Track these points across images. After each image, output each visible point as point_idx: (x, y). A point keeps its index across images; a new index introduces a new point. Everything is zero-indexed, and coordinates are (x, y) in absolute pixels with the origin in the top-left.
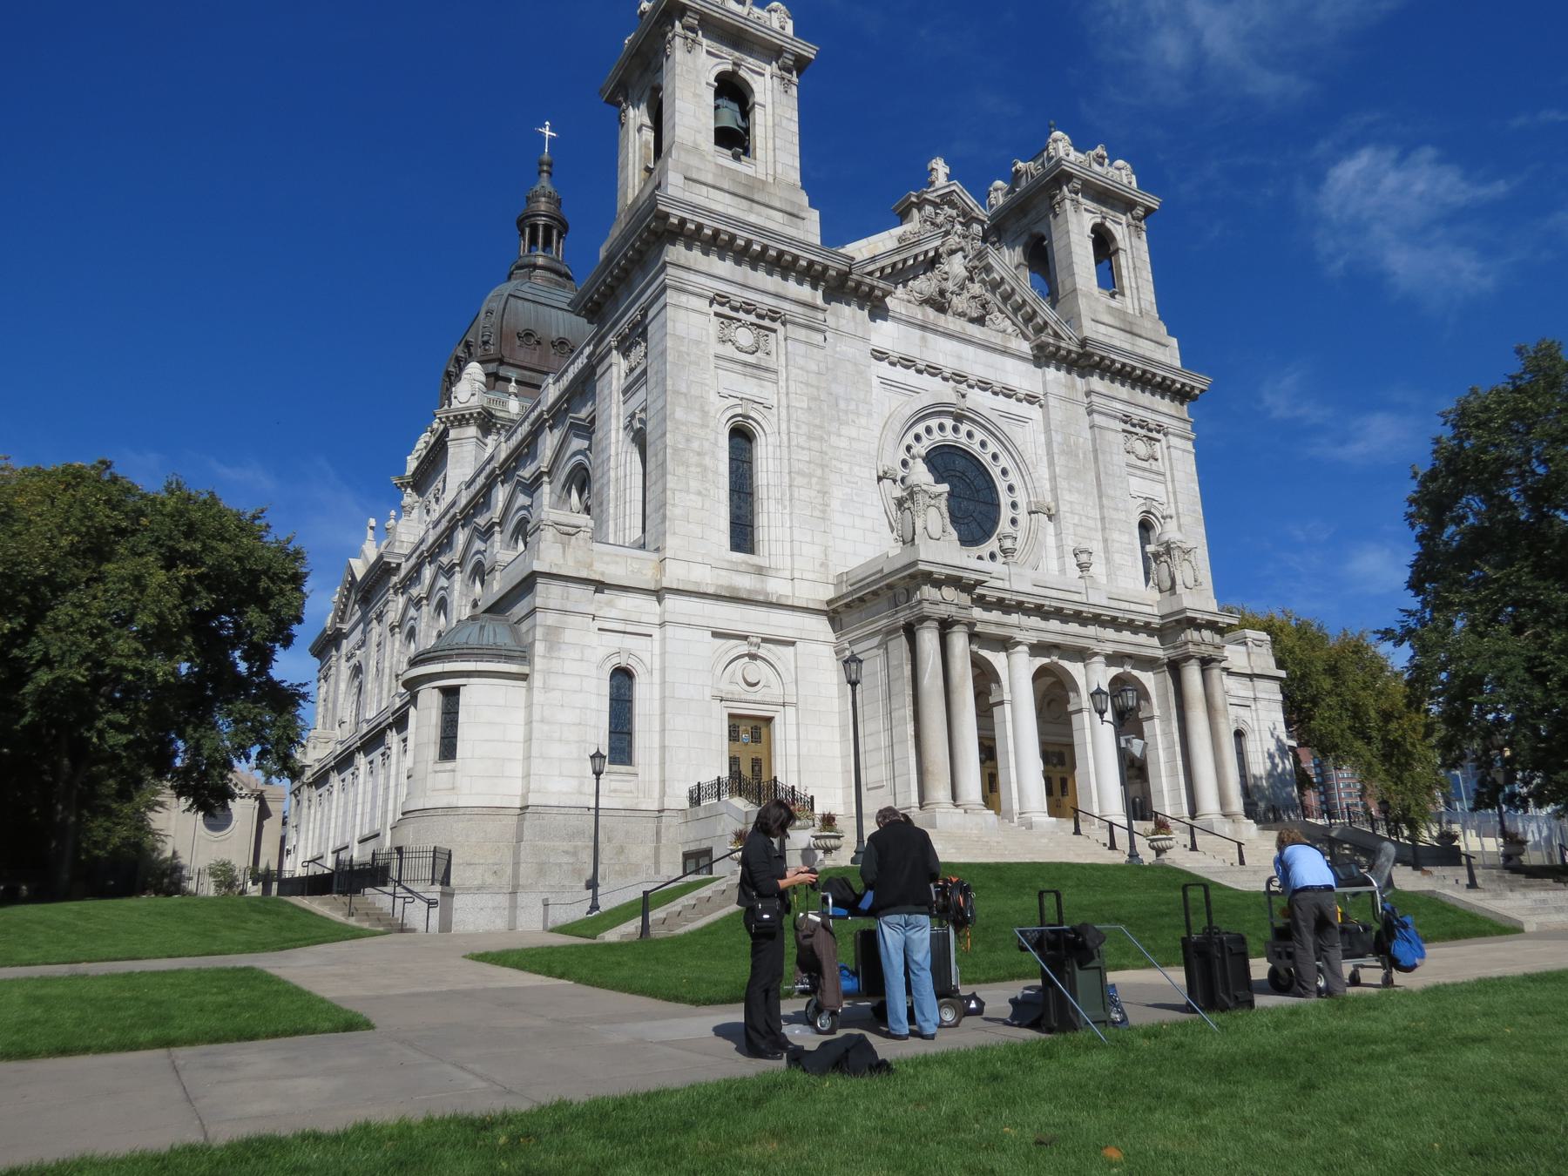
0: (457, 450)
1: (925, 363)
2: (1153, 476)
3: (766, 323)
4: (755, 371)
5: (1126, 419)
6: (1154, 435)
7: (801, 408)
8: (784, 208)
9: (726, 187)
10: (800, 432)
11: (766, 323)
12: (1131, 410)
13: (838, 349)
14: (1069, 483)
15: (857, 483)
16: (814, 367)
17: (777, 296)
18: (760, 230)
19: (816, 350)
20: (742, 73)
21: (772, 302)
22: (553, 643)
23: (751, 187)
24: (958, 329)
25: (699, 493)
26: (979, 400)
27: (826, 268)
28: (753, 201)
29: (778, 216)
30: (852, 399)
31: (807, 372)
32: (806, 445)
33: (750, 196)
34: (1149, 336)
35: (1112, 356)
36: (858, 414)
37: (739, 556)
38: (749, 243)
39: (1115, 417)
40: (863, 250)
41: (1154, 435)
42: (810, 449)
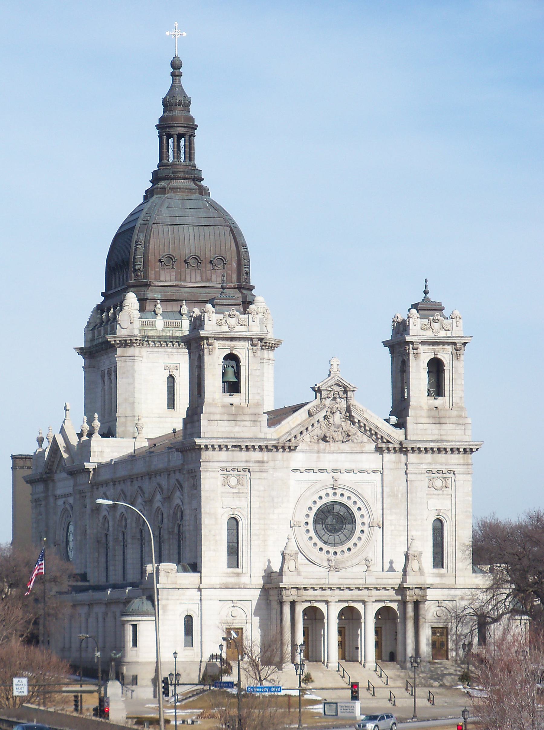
0: (123, 364)
3: (242, 473)
5: (429, 471)
6: (448, 475)
11: (242, 473)
12: (433, 466)
13: (275, 475)
16: (262, 488)
20: (234, 352)
21: (244, 465)
22: (165, 611)
25: (214, 550)
26: (345, 479)
34: (451, 423)
35: (418, 446)
37: (231, 570)
41: (448, 475)
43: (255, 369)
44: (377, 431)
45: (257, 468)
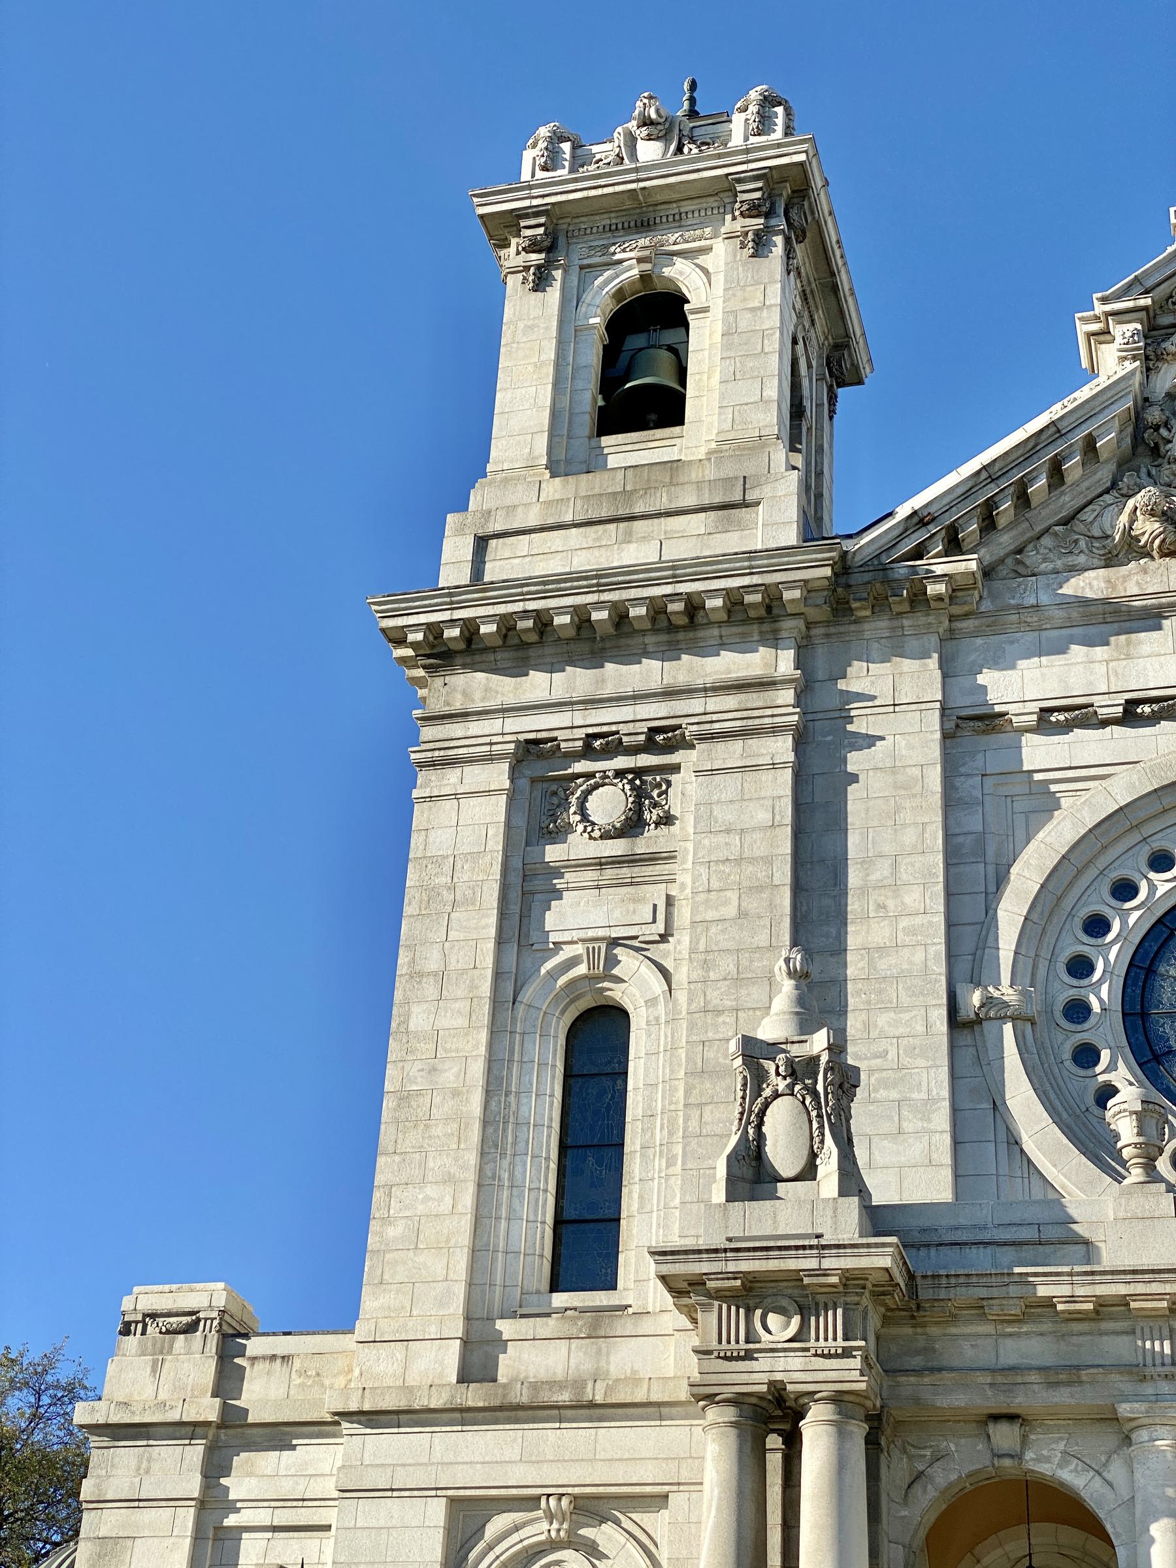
1: (1121, 699)
4: (625, 872)
8: (706, 500)
9: (568, 518)
10: (712, 975)
17: (670, 693)
18: (599, 579)
19: (766, 777)
23: (626, 495)
28: (632, 518)
29: (697, 522)
33: (621, 512)
43: (753, 310)
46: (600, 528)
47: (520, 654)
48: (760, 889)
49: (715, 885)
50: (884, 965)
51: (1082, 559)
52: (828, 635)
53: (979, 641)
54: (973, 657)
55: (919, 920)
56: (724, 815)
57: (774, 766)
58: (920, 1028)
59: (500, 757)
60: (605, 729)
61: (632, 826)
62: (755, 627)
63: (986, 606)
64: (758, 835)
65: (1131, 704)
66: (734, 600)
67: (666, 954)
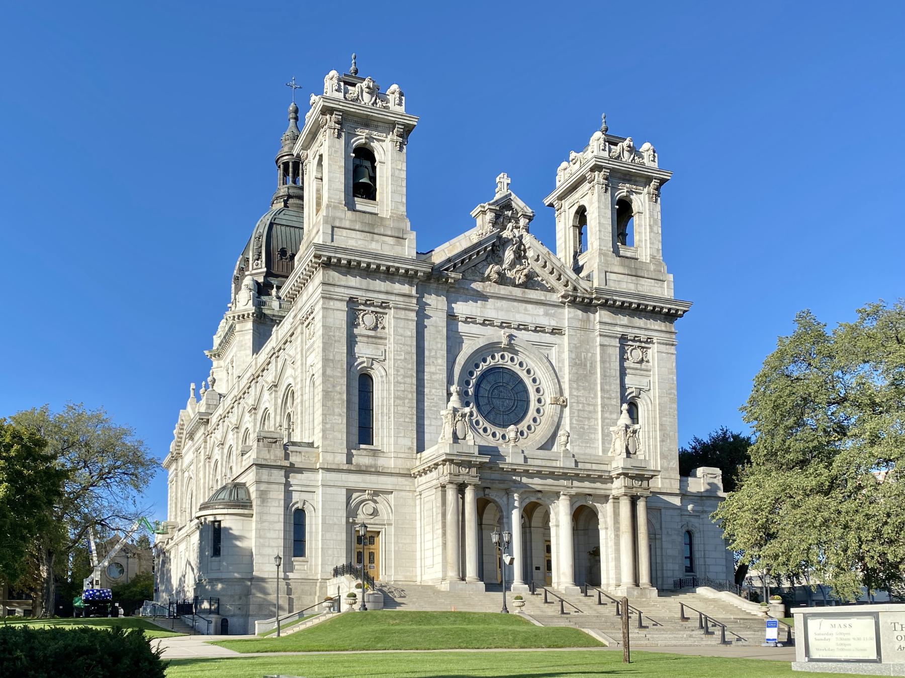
2: (642, 372)
4: (374, 340)
7: (400, 360)
9: (357, 228)
12: (630, 330)
14: (577, 384)
15: (433, 399)
16: (409, 333)
17: (387, 293)
18: (376, 256)
19: (410, 323)
21: (383, 297)
24: (507, 293)
27: (416, 272)
28: (374, 233)
30: (433, 349)
31: (405, 337)
32: (402, 381)
33: (371, 231)
36: (436, 358)
38: (369, 265)
39: (616, 337)
40: (446, 250)
41: (647, 345)
42: (404, 383)
44: (562, 273)
45: (402, 303)
46: (365, 234)
47: (349, 270)
48: (409, 353)
49: (399, 350)
50: (434, 377)
51: (477, 278)
52: (422, 285)
53: (453, 295)
54: (452, 299)
55: (441, 367)
56: (400, 331)
57: (412, 320)
58: (441, 394)
59: (344, 301)
60: (370, 299)
61: (375, 328)
62: (408, 279)
63: (457, 286)
64: (408, 338)
65: (485, 320)
66: (407, 271)
67: (385, 365)
